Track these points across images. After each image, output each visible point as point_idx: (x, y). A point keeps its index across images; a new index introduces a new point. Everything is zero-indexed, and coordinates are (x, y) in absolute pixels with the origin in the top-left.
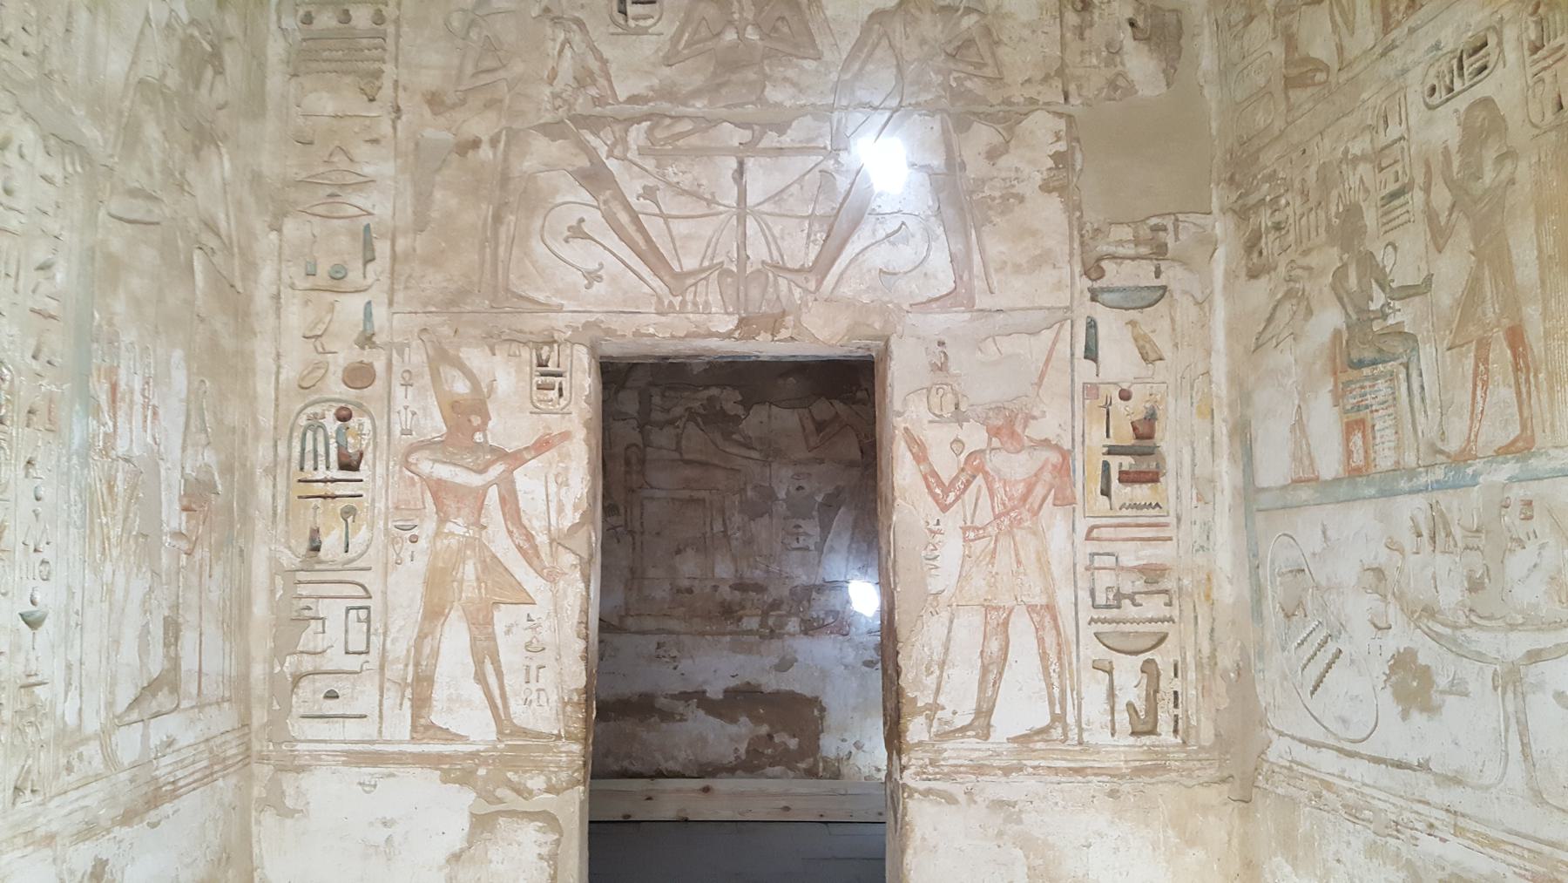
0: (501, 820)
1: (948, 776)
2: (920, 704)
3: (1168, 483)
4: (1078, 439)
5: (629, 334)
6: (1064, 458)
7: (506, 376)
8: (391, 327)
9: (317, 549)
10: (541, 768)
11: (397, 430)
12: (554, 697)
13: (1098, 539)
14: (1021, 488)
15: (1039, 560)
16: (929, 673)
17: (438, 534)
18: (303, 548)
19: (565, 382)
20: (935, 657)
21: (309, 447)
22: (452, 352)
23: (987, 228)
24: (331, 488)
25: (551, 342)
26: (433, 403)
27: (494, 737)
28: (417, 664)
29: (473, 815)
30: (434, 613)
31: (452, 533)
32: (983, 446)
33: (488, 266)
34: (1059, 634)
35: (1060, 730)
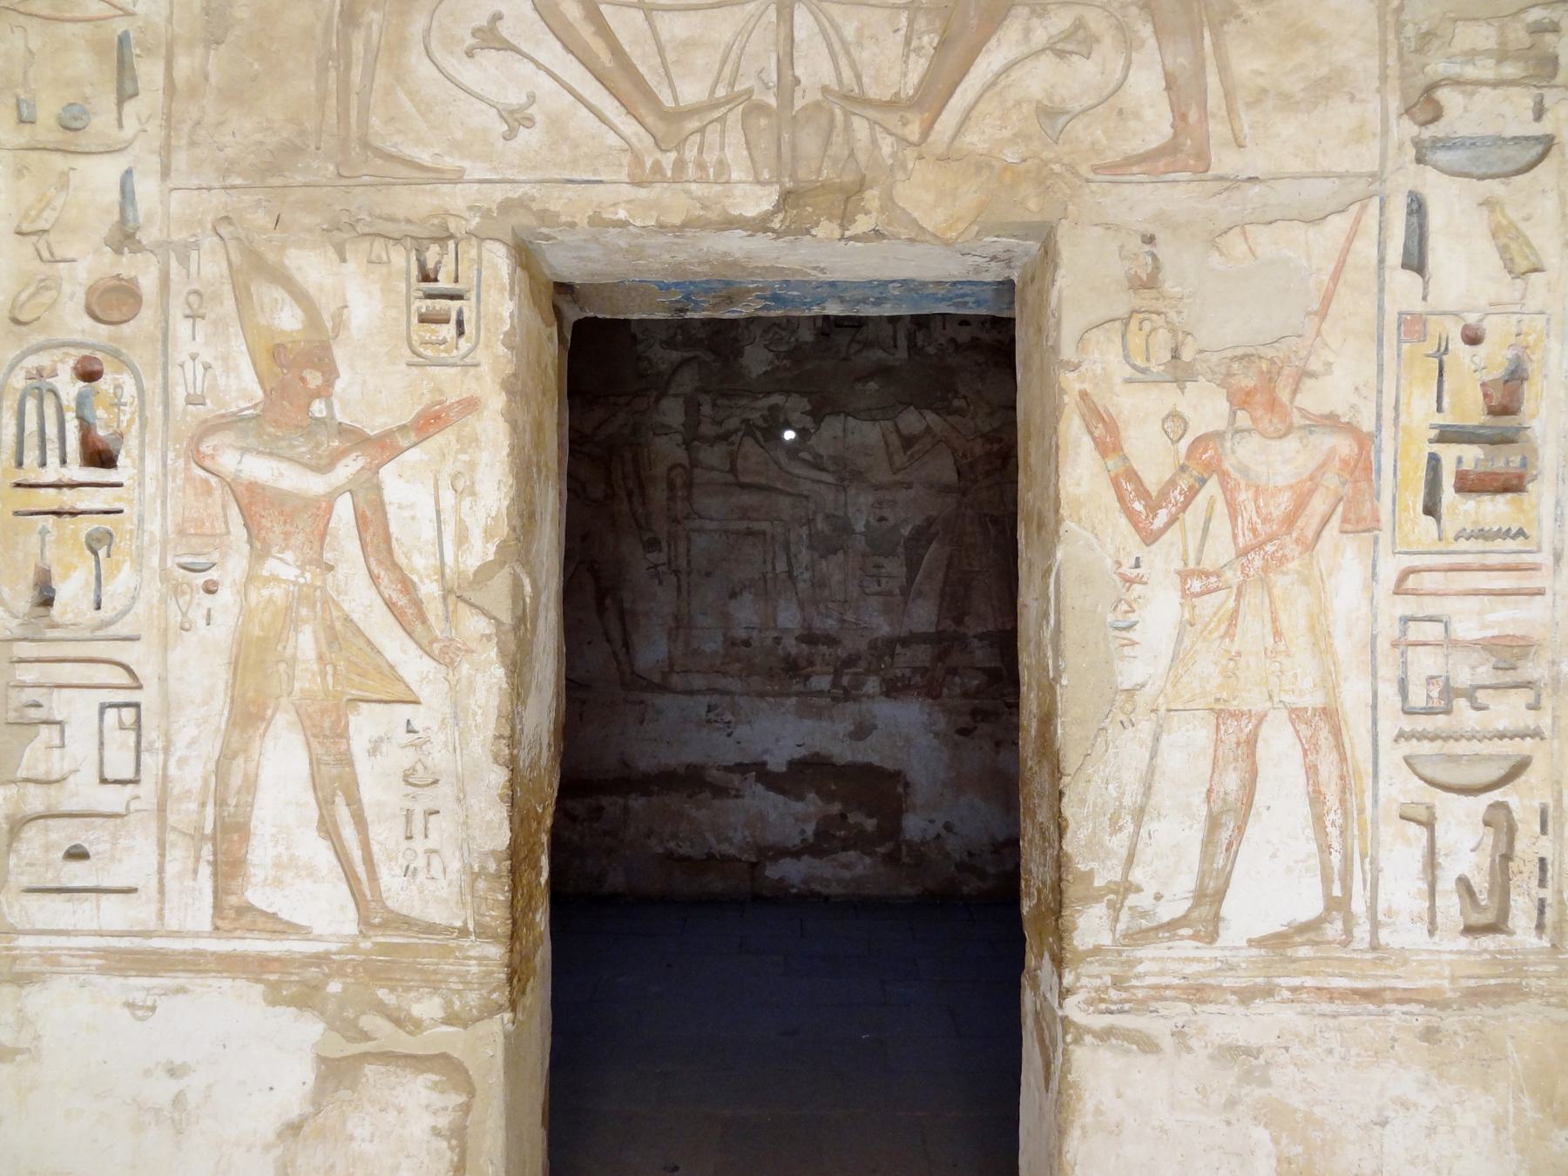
0: (370, 1070)
1: (1142, 1006)
2: (1099, 882)
3: (1542, 494)
4: (1388, 414)
5: (582, 221)
6: (1361, 447)
7: (362, 297)
8: (167, 215)
9: (47, 602)
10: (433, 983)
11: (179, 395)
12: (455, 865)
13: (1414, 593)
14: (1284, 502)
15: (1312, 628)
16: (1116, 828)
17: (250, 579)
18: (24, 599)
19: (468, 307)
20: (1128, 801)
21: (31, 424)
22: (271, 257)
23: (1232, 27)
24: (68, 499)
25: (443, 238)
26: (239, 347)
27: (352, 928)
28: (220, 803)
29: (322, 1060)
30: (247, 716)
31: (275, 579)
32: (1221, 425)
33: (333, 102)
34: (1343, 759)
35: (1339, 925)
